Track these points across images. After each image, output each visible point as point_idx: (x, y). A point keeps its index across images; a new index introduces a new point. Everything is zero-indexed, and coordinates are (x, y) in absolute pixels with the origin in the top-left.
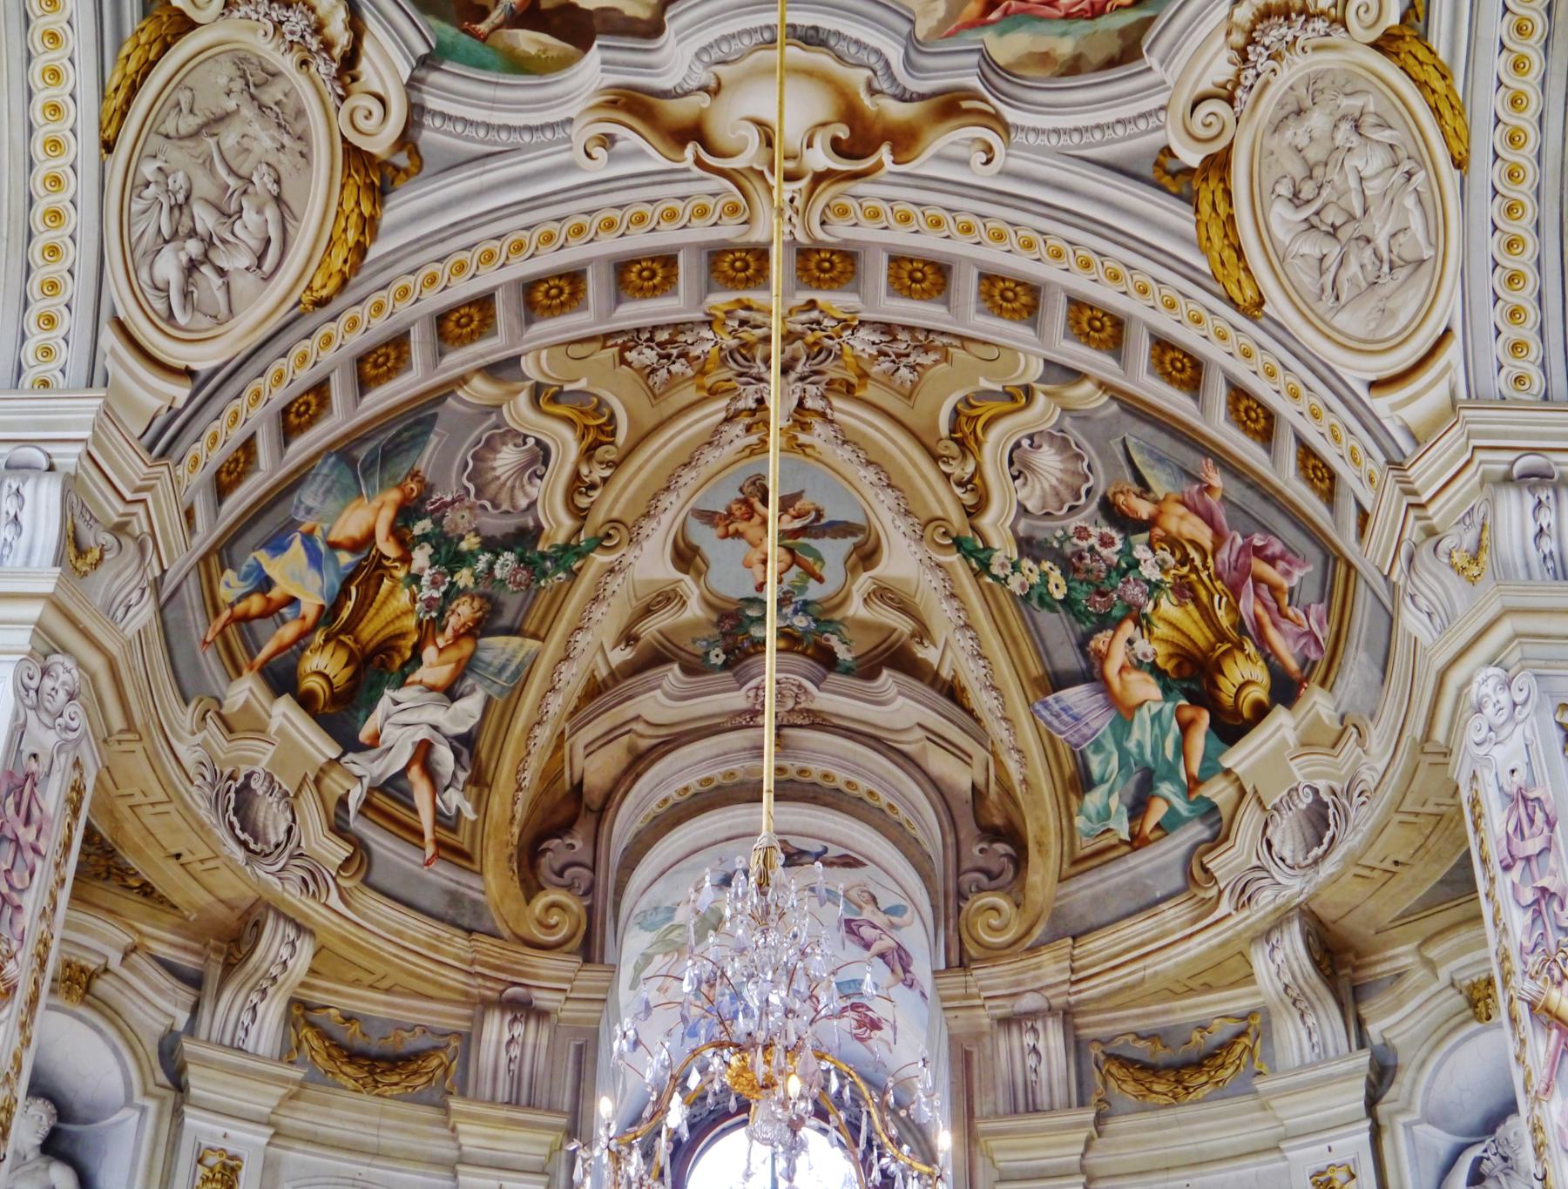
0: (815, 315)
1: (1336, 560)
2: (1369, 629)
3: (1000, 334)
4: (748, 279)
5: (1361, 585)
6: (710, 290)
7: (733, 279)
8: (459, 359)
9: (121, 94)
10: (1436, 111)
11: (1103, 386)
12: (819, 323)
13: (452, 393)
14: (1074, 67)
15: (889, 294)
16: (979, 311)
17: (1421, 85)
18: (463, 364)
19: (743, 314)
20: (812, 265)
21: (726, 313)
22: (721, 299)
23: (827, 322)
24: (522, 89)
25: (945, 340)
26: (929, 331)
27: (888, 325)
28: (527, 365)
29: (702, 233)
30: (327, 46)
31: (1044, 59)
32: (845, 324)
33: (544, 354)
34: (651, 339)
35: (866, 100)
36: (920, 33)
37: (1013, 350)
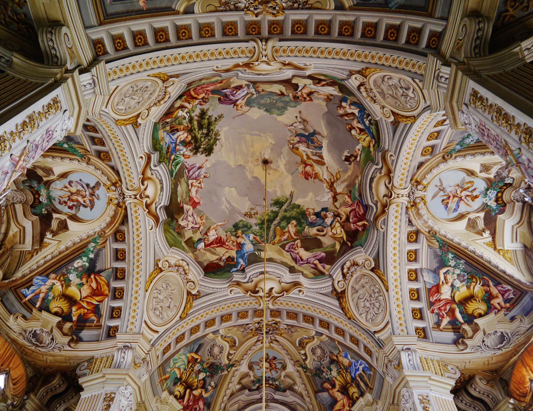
0: (256, 12)
1: (105, 19)
2: (87, 9)
3: (207, 17)
4: (273, 24)
5: (96, 24)
6: (283, 21)
7: (277, 24)
8: (349, 17)
9: (409, 119)
10: (125, 120)
11: (177, 13)
12: (255, 9)
13: (354, 5)
14: (201, 80)
15: (237, 22)
16: (214, 23)
17: (130, 118)
18: (349, 15)
19: (275, 12)
20: (257, 29)
21: (278, 13)
22: (280, 18)
23: (252, 9)
24: (324, 73)
25: (221, 8)
26: (226, 11)
27: (236, 10)
28: (333, 6)
29: (285, 44)
30: (365, 88)
31: (207, 79)
32: (247, 8)
33: (328, 8)
34: (299, 4)
35: (246, 69)
36: (235, 77)
37: (204, 13)
